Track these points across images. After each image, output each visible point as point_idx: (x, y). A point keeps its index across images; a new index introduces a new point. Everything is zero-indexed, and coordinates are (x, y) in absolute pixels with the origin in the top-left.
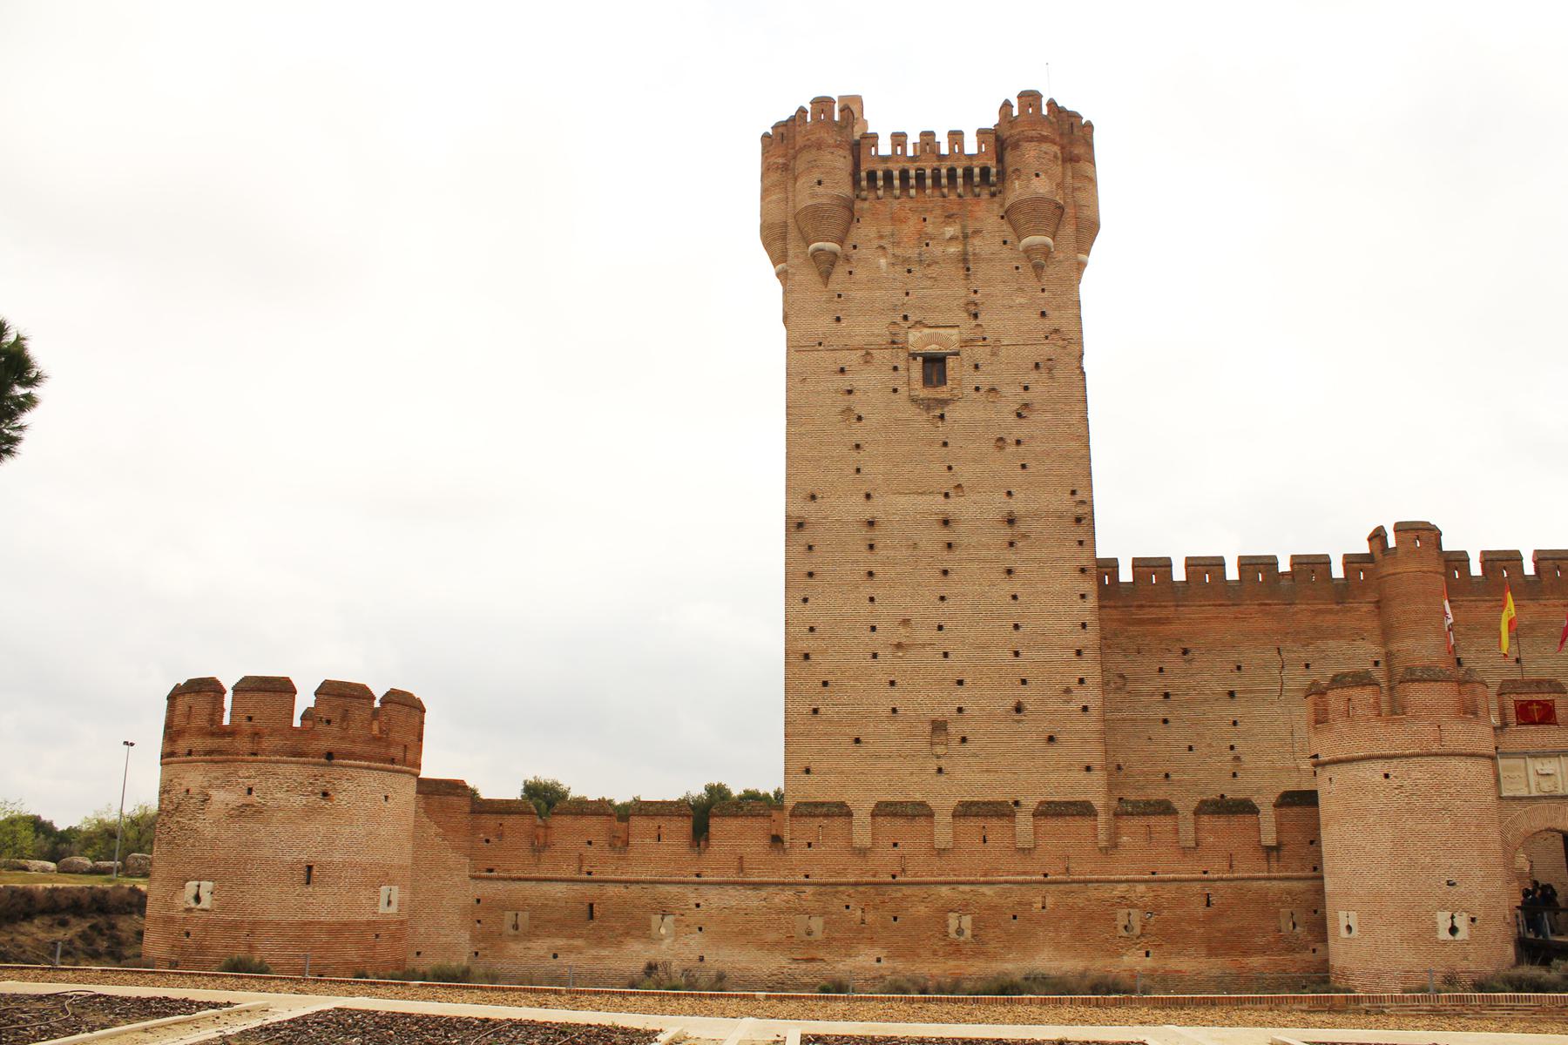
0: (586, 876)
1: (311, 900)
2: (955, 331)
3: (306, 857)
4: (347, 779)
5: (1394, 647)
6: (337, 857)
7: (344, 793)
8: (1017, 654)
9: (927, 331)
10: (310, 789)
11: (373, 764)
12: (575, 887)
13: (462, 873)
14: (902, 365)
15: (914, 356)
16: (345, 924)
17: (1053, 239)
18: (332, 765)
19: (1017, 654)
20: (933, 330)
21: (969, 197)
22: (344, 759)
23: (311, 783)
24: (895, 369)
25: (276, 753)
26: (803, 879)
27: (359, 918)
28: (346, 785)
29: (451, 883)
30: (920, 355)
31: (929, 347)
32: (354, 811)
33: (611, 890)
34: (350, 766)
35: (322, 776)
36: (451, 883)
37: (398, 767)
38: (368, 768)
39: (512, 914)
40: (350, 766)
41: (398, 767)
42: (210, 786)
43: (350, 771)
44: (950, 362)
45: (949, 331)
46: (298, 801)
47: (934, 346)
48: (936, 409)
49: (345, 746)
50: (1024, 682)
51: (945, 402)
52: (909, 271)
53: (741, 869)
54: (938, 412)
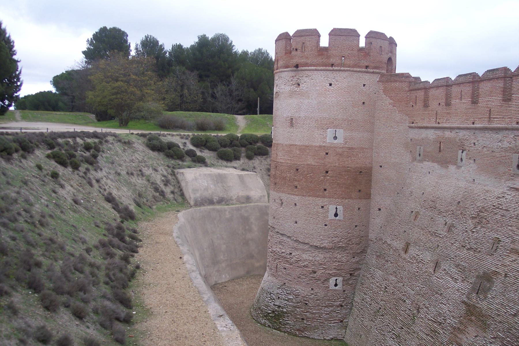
0: (437, 125)
1: (292, 134)
3: (290, 114)
4: (306, 77)
6: (302, 115)
7: (305, 83)
10: (291, 83)
11: (318, 68)
12: (436, 132)
13: (405, 125)
16: (308, 147)
18: (299, 71)
22: (303, 67)
23: (292, 80)
25: (281, 67)
27: (314, 144)
28: (305, 79)
29: (397, 130)
32: (310, 92)
33: (448, 134)
34: (306, 70)
35: (295, 76)
36: (397, 130)
37: (337, 68)
38: (316, 70)
39: (419, 147)
40: (306, 70)
41: (337, 68)
43: (310, 73)
46: (288, 89)
49: (303, 61)
53: (490, 119)
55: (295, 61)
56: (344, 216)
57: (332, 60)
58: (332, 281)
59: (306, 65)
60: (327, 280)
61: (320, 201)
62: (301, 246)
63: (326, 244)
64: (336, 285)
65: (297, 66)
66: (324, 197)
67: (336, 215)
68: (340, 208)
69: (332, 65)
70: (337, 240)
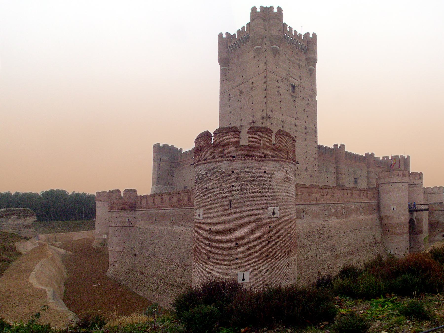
2: (297, 81)
5: (338, 166)
8: (306, 157)
9: (292, 79)
14: (288, 85)
15: (290, 84)
19: (306, 157)
20: (293, 79)
21: (300, 51)
24: (287, 85)
26: (337, 202)
30: (291, 84)
31: (293, 83)
42: (274, 170)
44: (296, 88)
45: (296, 81)
47: (294, 83)
50: (307, 164)
51: (296, 97)
52: (290, 63)
54: (294, 99)
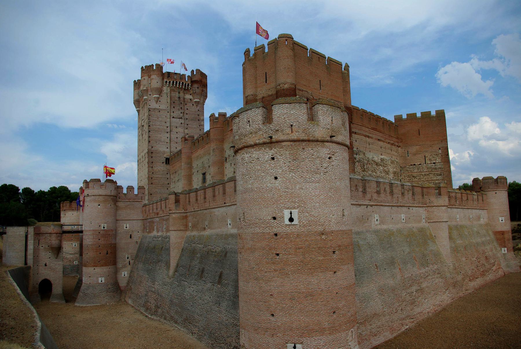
6: (66, 222)
17: (147, 96)
48: (142, 135)
55: (64, 209)
56: (77, 246)
57: (73, 209)
58: (75, 262)
59: (67, 210)
60: (74, 262)
61: (71, 243)
62: (67, 254)
63: (73, 253)
64: (76, 263)
65: (65, 210)
66: (72, 241)
67: (75, 245)
68: (76, 244)
69: (73, 210)
70: (76, 251)
